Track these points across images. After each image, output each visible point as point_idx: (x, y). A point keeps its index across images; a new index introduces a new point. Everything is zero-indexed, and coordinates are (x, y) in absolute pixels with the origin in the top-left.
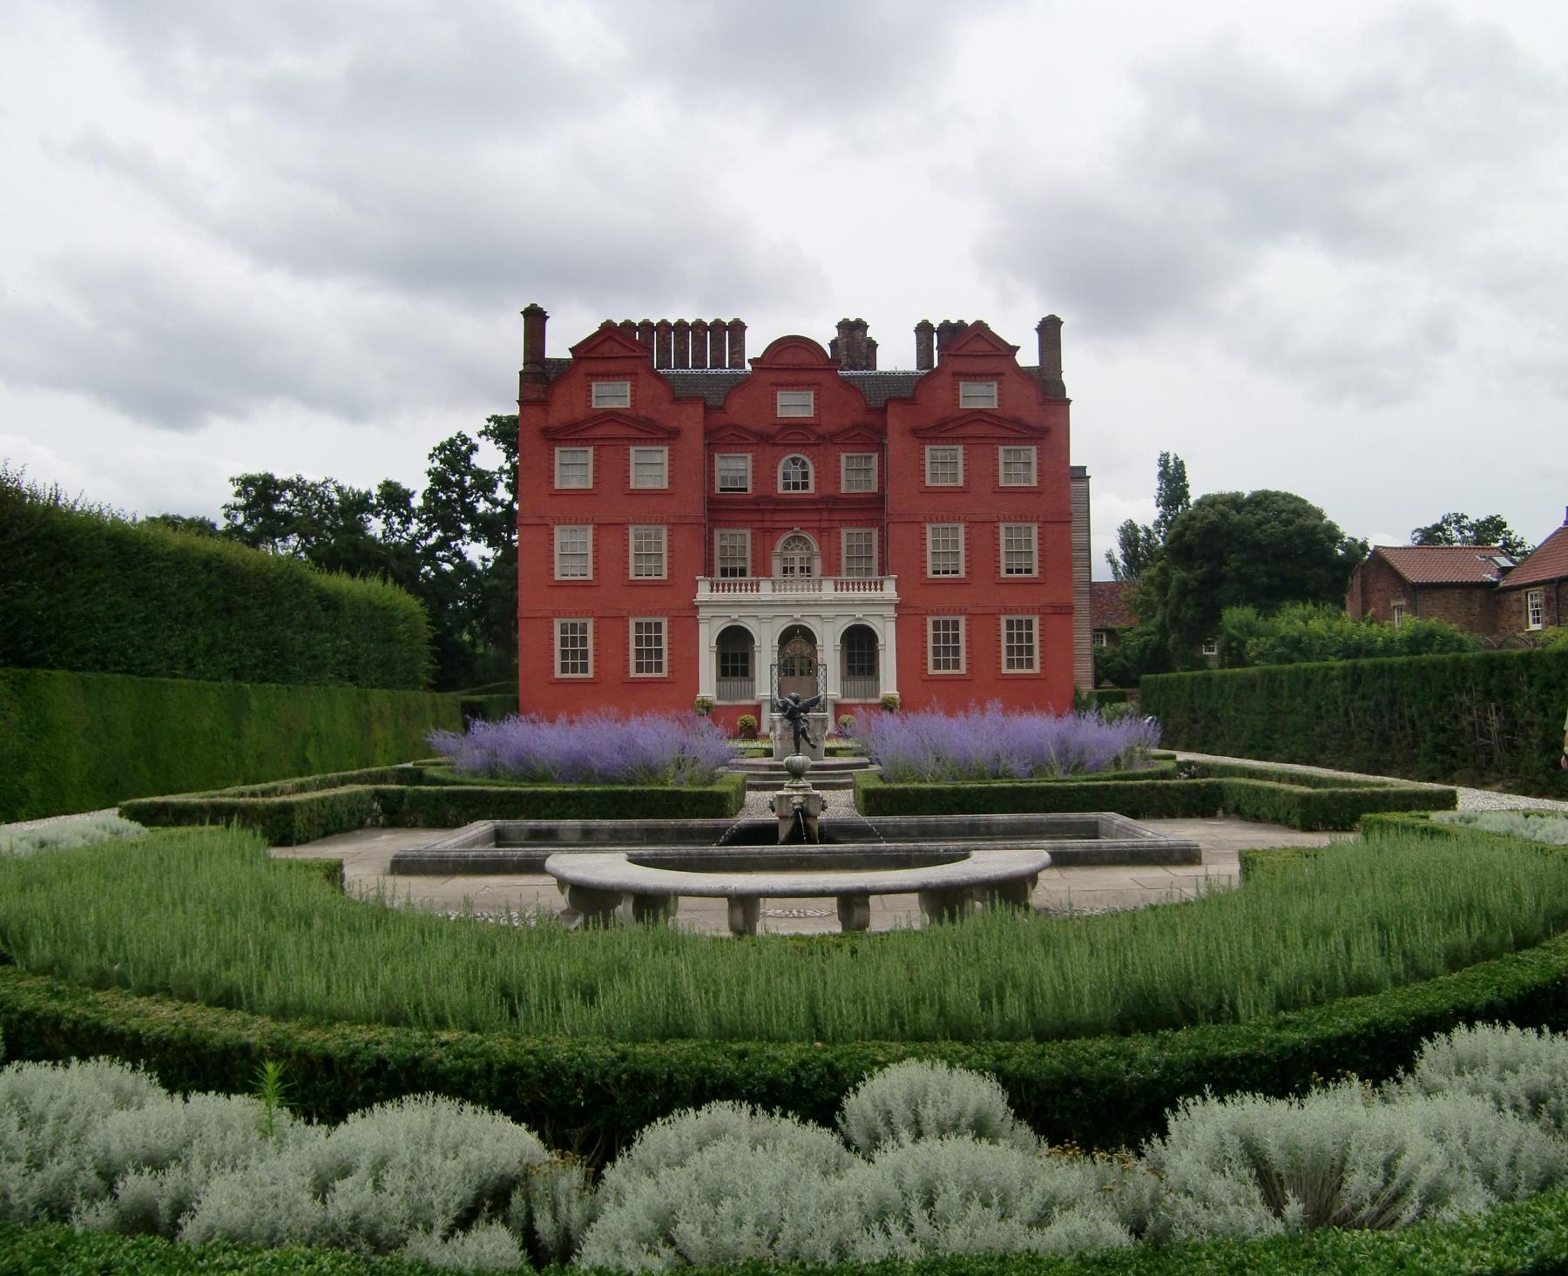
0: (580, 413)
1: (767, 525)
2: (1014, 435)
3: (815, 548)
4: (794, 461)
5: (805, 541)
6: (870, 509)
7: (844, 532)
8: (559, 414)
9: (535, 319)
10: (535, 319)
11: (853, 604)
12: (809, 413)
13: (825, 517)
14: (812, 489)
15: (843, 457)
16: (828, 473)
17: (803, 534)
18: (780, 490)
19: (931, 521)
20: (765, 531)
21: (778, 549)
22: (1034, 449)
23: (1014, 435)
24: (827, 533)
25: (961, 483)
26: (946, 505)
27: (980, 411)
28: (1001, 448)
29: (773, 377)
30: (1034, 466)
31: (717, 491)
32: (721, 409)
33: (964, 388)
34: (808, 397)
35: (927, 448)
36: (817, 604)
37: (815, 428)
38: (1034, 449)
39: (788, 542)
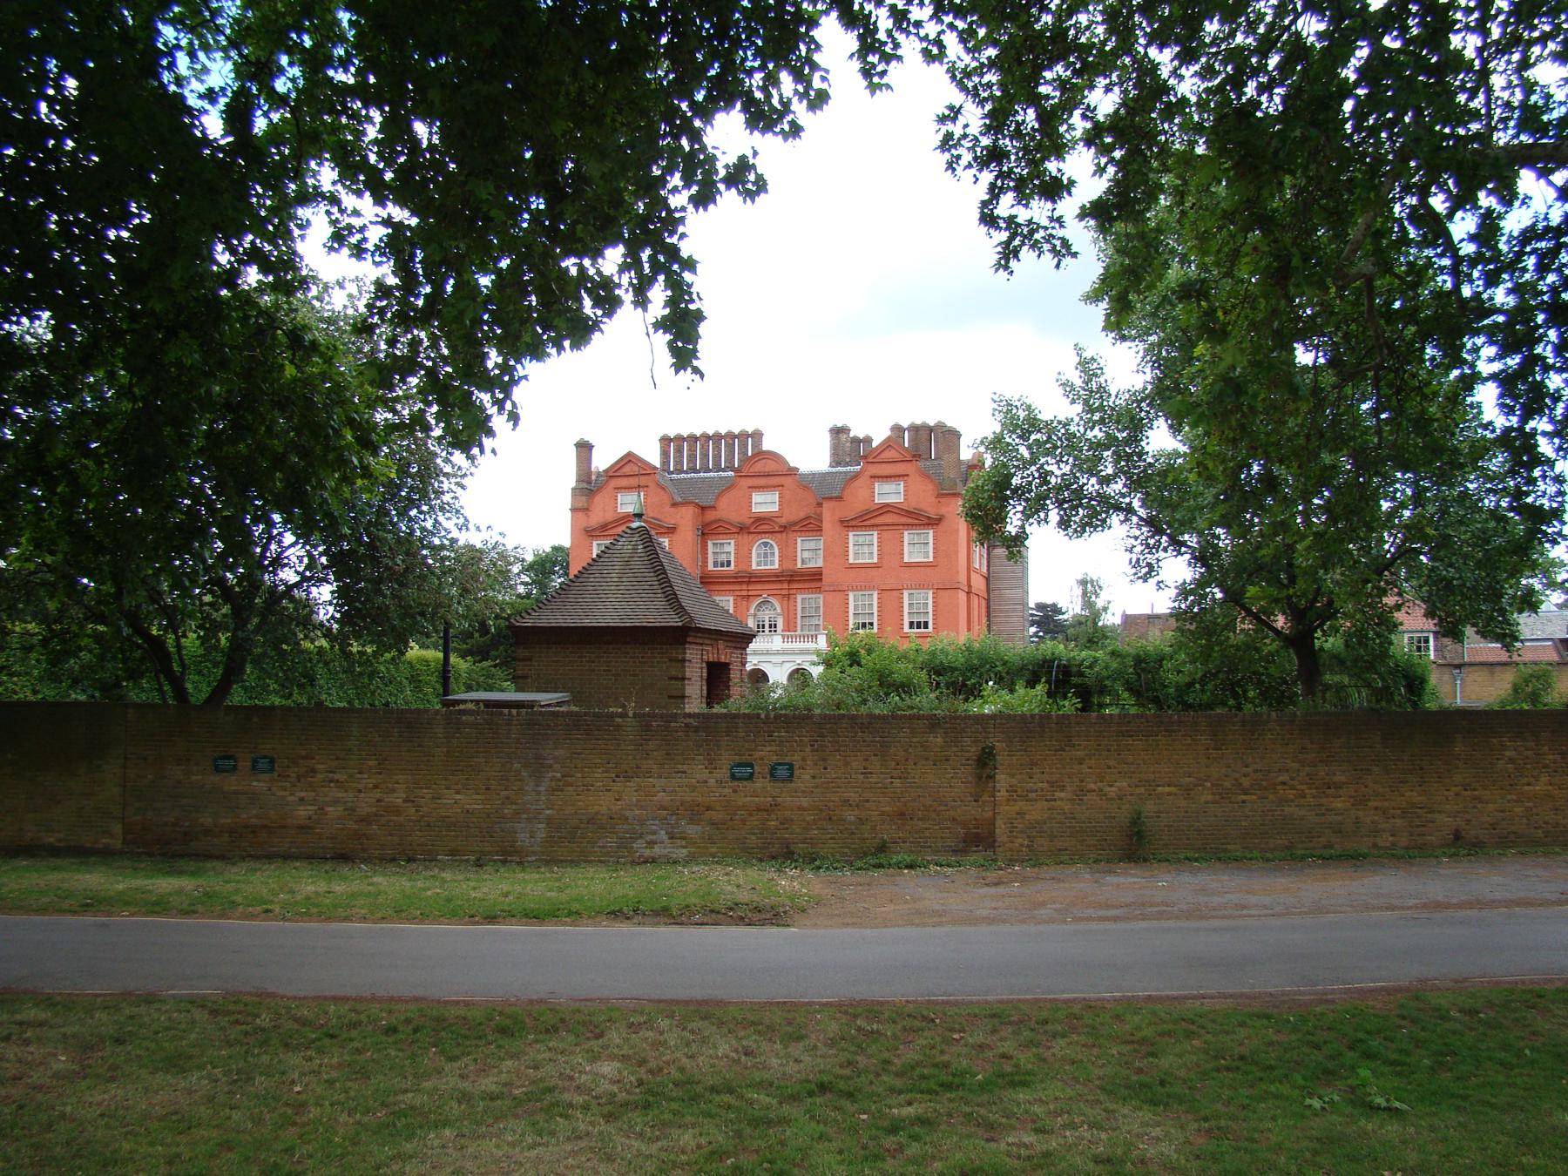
0: (610, 517)
1: (745, 593)
2: (916, 522)
3: (779, 610)
4: (766, 544)
5: (773, 605)
6: (813, 579)
7: (799, 598)
8: (596, 518)
9: (584, 448)
10: (584, 448)
11: (793, 652)
12: (775, 508)
13: (785, 586)
14: (776, 566)
15: (799, 540)
16: (788, 553)
17: (771, 599)
18: (754, 567)
19: (853, 590)
20: (743, 597)
21: (752, 611)
22: (931, 532)
23: (916, 522)
24: (787, 597)
25: (875, 560)
26: (864, 576)
27: (888, 505)
28: (906, 533)
29: (751, 482)
30: (931, 545)
31: (711, 567)
32: (713, 507)
33: (879, 487)
34: (773, 497)
35: (851, 534)
36: (768, 653)
37: (778, 520)
38: (931, 532)
39: (760, 605)
